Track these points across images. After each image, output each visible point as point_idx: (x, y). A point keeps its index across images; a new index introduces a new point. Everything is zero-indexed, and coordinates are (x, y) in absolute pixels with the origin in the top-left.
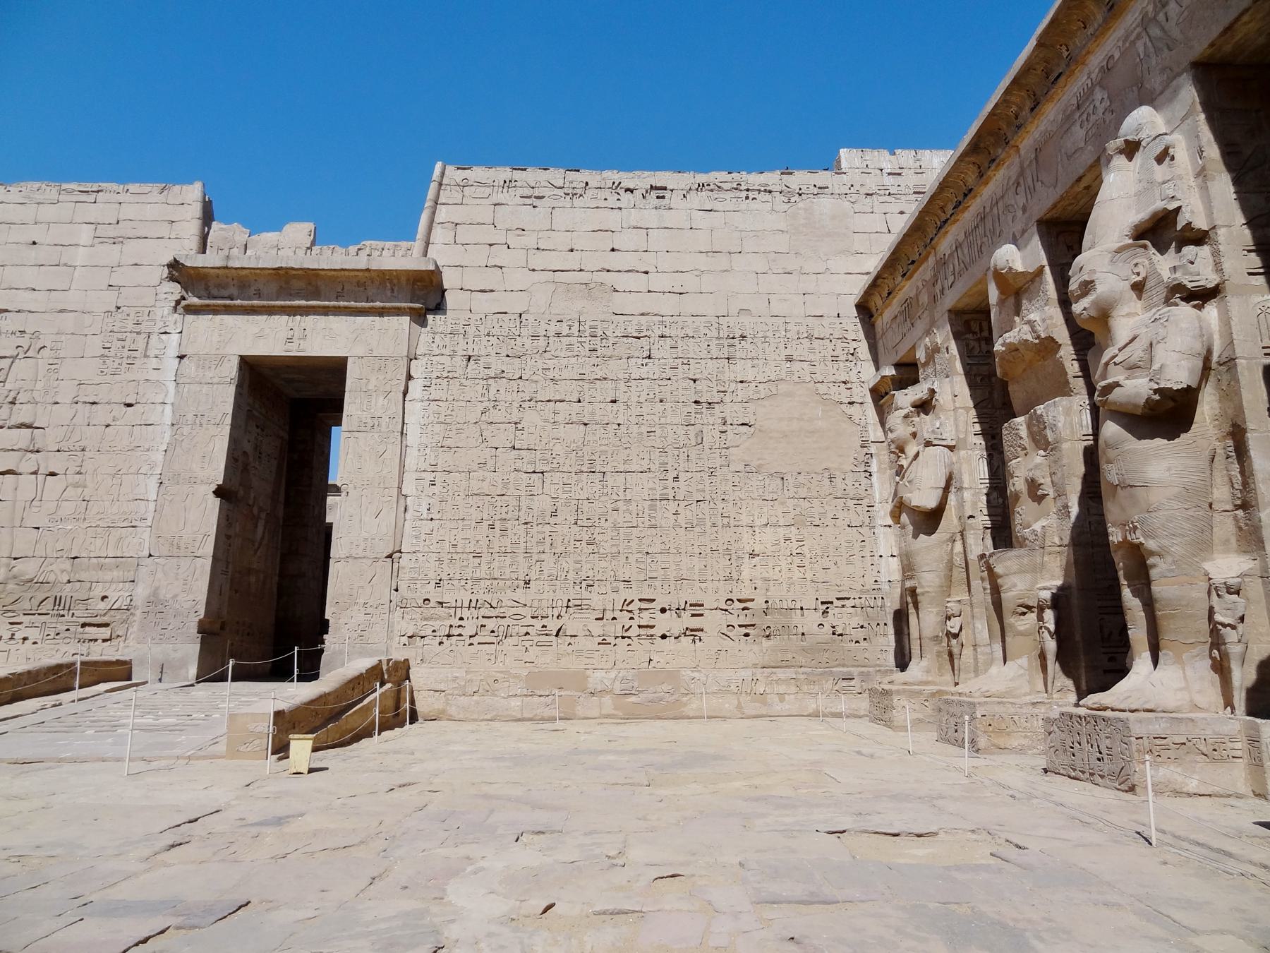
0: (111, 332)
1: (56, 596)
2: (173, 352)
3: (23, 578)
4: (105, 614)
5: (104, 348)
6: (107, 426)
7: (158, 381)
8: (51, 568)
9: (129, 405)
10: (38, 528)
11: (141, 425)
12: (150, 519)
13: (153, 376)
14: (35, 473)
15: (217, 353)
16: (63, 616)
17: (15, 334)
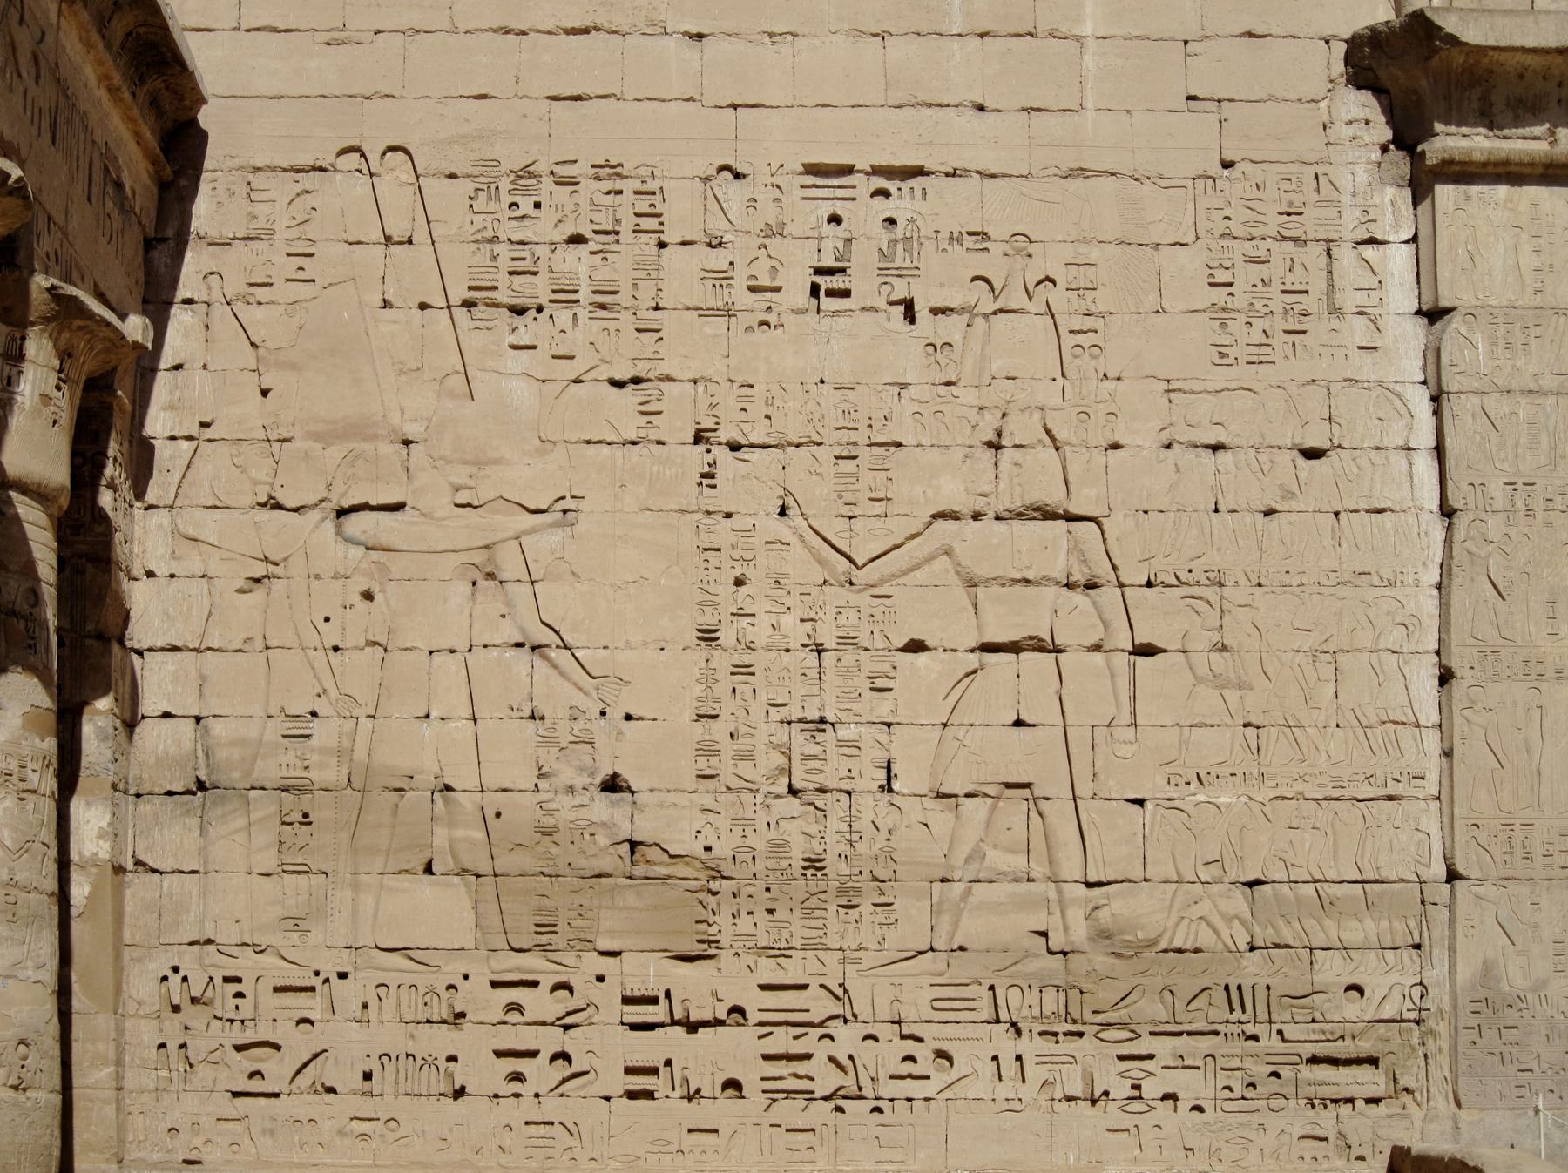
0: (1223, 236)
1: (1227, 988)
2: (1402, 298)
3: (1127, 937)
4: (1362, 1032)
5: (1211, 284)
6: (1269, 512)
7: (1380, 384)
8: (1196, 911)
9: (1312, 454)
10: (1140, 802)
11: (1356, 511)
12: (1433, 777)
13: (1366, 368)
14: (1096, 648)
15: (1538, 301)
16: (1255, 1038)
17: (961, 243)
